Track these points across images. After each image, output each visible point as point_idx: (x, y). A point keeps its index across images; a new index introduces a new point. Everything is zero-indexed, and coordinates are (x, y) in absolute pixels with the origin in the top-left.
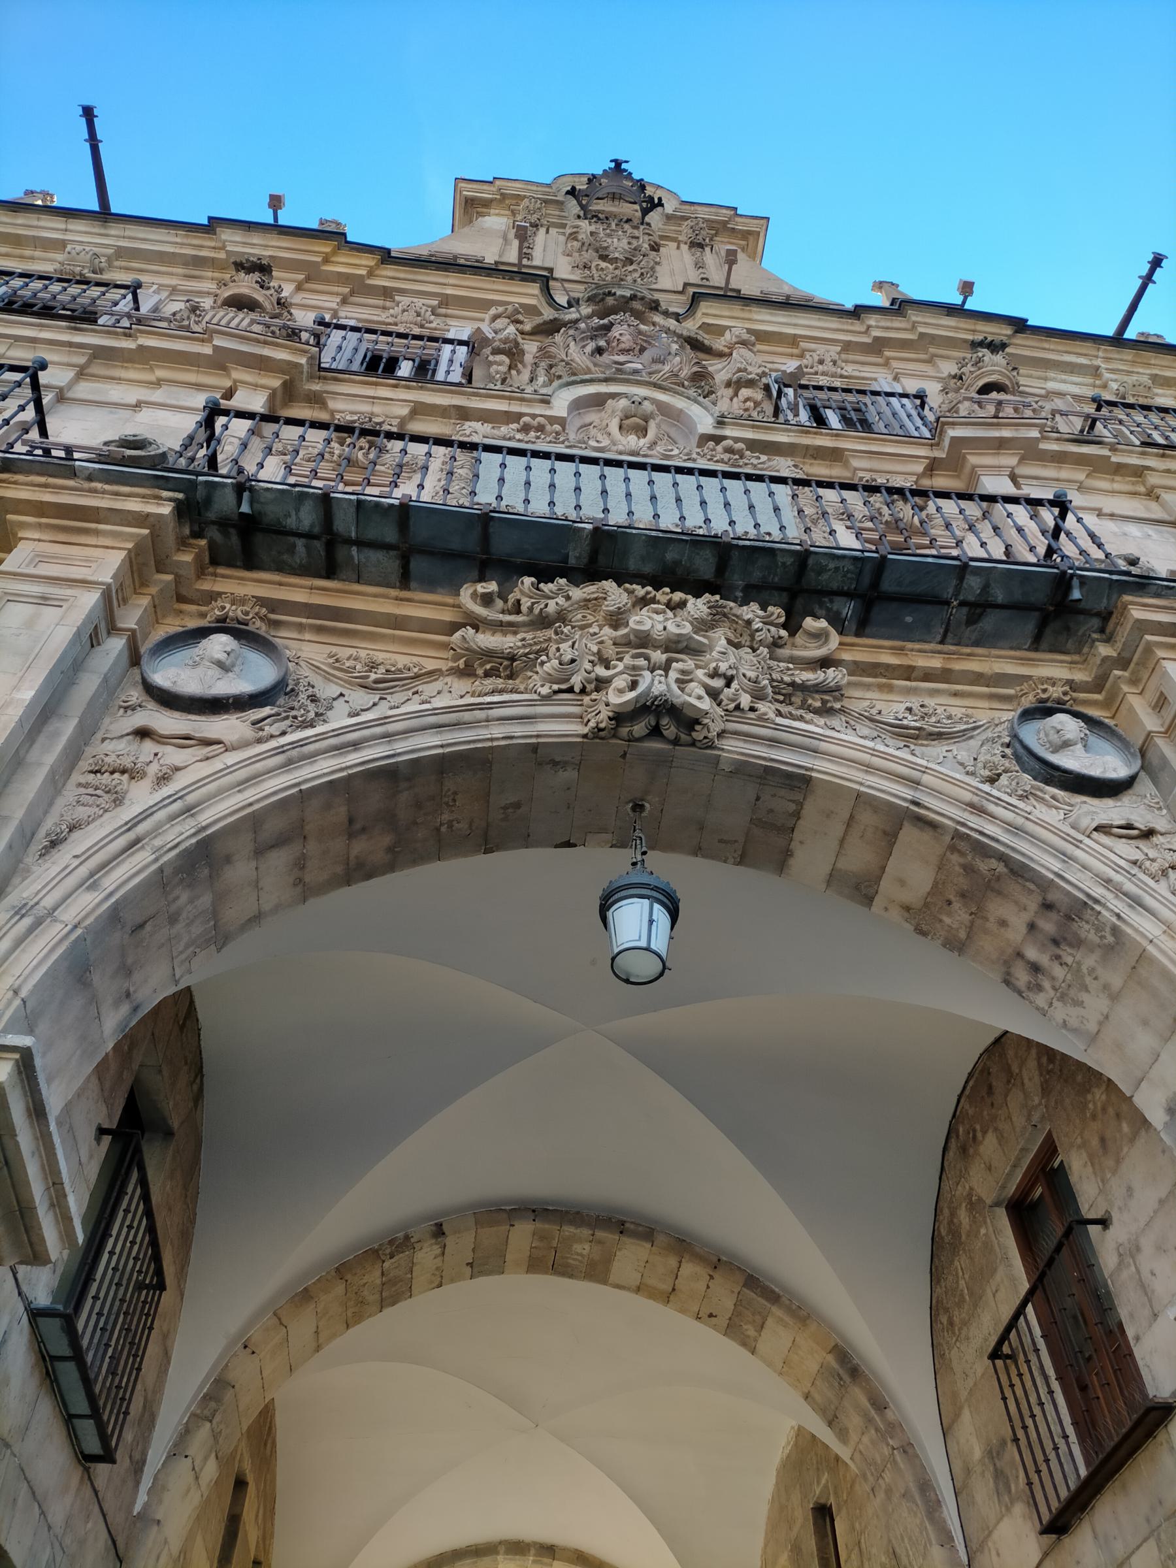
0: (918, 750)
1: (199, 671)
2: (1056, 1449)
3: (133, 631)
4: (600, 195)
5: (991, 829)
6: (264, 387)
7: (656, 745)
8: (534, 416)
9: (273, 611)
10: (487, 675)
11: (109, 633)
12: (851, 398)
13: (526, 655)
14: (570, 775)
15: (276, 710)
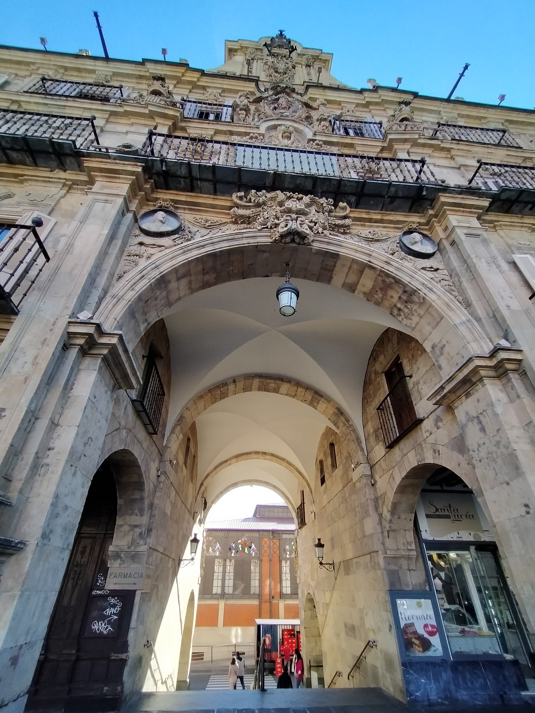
0: (371, 245)
1: (156, 223)
2: (392, 430)
3: (134, 211)
4: (275, 46)
5: (391, 269)
6: (166, 125)
7: (294, 245)
8: (254, 133)
9: (176, 204)
10: (242, 223)
11: (127, 212)
12: (358, 125)
13: (253, 216)
14: (267, 255)
15: (179, 236)
